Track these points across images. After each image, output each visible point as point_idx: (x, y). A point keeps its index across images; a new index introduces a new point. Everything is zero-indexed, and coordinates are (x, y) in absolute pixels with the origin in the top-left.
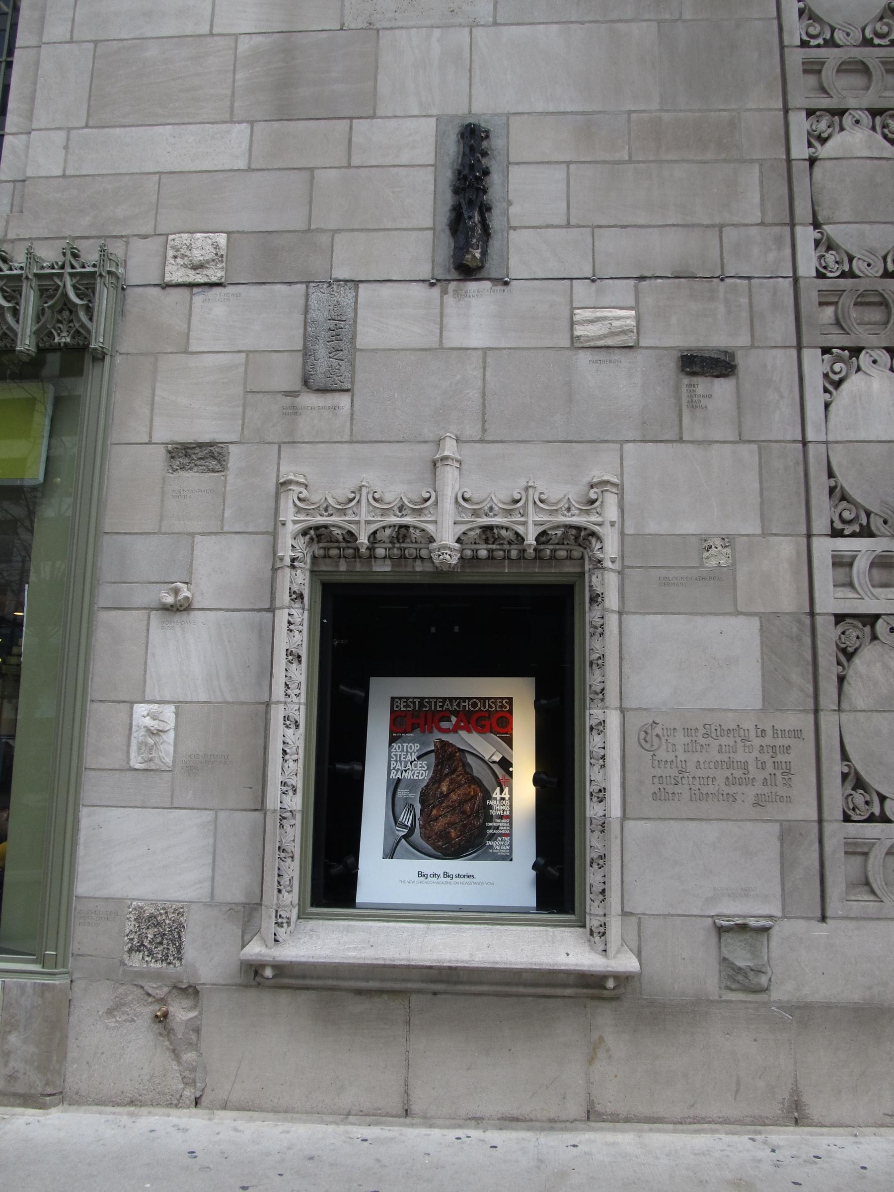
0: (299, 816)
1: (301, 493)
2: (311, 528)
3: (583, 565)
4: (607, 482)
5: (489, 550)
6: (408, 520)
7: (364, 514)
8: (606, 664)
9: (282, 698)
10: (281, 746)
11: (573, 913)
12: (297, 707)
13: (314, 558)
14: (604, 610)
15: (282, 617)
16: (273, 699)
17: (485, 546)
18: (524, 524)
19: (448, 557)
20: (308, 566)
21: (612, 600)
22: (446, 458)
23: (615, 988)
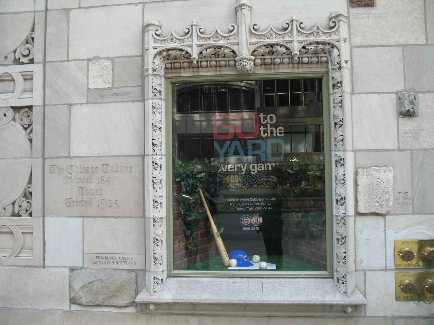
0: (164, 220)
1: (157, 30)
2: (163, 51)
3: (327, 67)
4: (341, 15)
5: (271, 59)
6: (221, 43)
7: (195, 41)
8: (345, 124)
9: (151, 152)
10: (151, 179)
11: (325, 270)
12: (160, 157)
13: (166, 68)
14: (342, 92)
15: (149, 103)
16: (146, 154)
17: (269, 57)
18: (291, 42)
19: (246, 63)
20: (163, 74)
21: (347, 86)
22: (244, 5)
23: (352, 312)
